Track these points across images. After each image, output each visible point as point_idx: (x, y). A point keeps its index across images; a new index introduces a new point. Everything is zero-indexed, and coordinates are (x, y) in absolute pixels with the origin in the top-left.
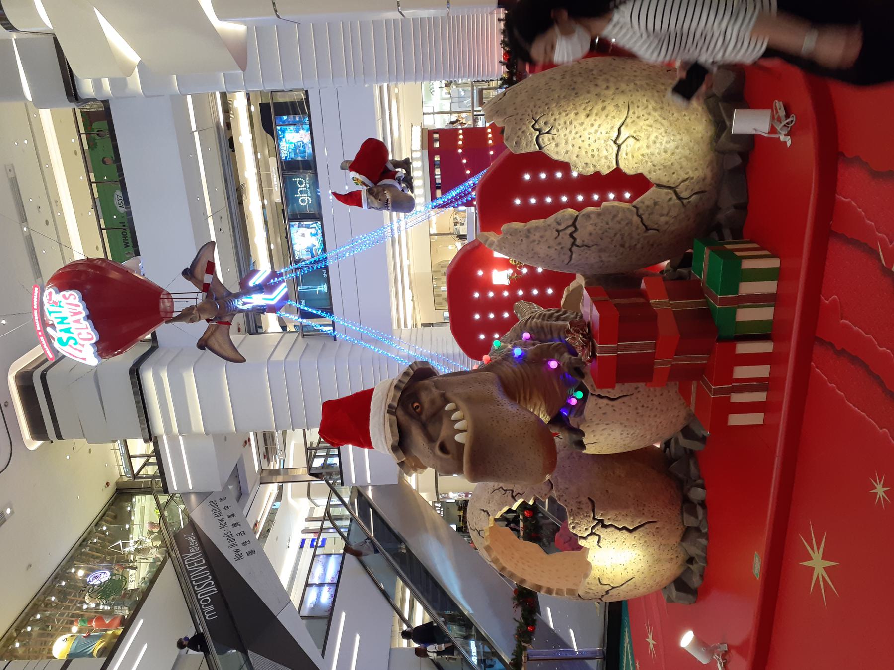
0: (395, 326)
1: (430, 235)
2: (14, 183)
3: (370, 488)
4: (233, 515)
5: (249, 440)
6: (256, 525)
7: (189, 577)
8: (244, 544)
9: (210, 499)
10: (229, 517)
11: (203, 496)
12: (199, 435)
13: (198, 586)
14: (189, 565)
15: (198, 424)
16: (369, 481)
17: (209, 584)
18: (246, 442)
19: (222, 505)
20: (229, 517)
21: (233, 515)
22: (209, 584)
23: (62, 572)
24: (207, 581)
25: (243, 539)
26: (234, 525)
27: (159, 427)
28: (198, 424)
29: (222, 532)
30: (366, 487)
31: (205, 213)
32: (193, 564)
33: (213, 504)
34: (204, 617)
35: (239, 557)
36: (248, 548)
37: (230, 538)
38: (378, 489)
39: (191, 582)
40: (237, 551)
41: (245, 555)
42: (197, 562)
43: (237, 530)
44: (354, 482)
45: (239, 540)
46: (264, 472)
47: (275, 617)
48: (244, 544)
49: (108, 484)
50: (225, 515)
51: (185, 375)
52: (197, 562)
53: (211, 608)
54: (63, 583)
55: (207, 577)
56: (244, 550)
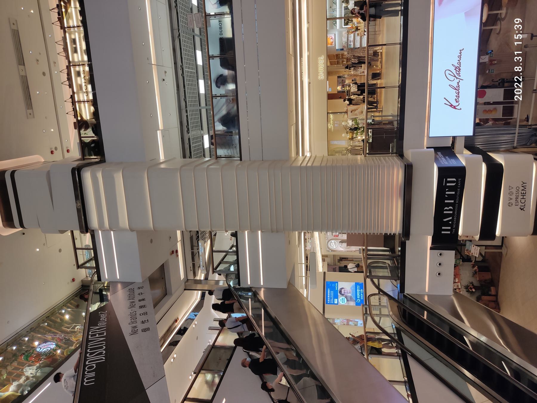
0: (293, 154)
1: (328, 113)
2: (16, 35)
3: (262, 290)
4: (143, 300)
5: (177, 251)
6: (176, 321)
7: (87, 345)
8: (143, 322)
9: (131, 287)
10: (140, 301)
11: (125, 284)
12: (124, 230)
13: (91, 354)
14: (92, 336)
15: (124, 221)
16: (262, 284)
17: (101, 354)
18: (173, 252)
19: (137, 292)
20: (140, 301)
21: (143, 300)
22: (101, 354)
23: (16, 339)
24: (100, 351)
25: (144, 318)
26: (141, 307)
27: (94, 223)
28: (124, 221)
29: (130, 311)
30: (260, 288)
31: (149, 59)
32: (95, 335)
33: (132, 291)
34: (83, 381)
35: (134, 332)
36: (145, 326)
37: (133, 317)
38: (268, 290)
39: (87, 349)
40: (135, 327)
41: (140, 331)
42: (99, 334)
43: (143, 310)
44: (249, 283)
45: (140, 319)
46: (189, 281)
47: (145, 390)
48: (143, 322)
49: (73, 280)
50: (136, 300)
51: (115, 175)
52: (99, 334)
53: (93, 374)
54: (14, 348)
55: (102, 347)
56: (140, 327)
